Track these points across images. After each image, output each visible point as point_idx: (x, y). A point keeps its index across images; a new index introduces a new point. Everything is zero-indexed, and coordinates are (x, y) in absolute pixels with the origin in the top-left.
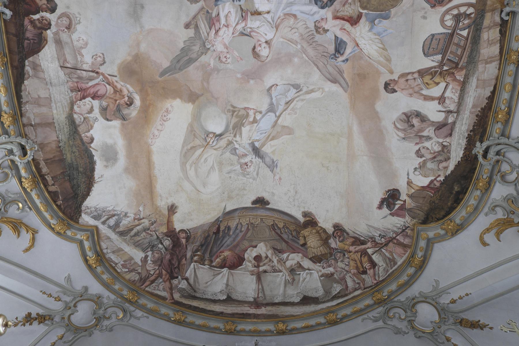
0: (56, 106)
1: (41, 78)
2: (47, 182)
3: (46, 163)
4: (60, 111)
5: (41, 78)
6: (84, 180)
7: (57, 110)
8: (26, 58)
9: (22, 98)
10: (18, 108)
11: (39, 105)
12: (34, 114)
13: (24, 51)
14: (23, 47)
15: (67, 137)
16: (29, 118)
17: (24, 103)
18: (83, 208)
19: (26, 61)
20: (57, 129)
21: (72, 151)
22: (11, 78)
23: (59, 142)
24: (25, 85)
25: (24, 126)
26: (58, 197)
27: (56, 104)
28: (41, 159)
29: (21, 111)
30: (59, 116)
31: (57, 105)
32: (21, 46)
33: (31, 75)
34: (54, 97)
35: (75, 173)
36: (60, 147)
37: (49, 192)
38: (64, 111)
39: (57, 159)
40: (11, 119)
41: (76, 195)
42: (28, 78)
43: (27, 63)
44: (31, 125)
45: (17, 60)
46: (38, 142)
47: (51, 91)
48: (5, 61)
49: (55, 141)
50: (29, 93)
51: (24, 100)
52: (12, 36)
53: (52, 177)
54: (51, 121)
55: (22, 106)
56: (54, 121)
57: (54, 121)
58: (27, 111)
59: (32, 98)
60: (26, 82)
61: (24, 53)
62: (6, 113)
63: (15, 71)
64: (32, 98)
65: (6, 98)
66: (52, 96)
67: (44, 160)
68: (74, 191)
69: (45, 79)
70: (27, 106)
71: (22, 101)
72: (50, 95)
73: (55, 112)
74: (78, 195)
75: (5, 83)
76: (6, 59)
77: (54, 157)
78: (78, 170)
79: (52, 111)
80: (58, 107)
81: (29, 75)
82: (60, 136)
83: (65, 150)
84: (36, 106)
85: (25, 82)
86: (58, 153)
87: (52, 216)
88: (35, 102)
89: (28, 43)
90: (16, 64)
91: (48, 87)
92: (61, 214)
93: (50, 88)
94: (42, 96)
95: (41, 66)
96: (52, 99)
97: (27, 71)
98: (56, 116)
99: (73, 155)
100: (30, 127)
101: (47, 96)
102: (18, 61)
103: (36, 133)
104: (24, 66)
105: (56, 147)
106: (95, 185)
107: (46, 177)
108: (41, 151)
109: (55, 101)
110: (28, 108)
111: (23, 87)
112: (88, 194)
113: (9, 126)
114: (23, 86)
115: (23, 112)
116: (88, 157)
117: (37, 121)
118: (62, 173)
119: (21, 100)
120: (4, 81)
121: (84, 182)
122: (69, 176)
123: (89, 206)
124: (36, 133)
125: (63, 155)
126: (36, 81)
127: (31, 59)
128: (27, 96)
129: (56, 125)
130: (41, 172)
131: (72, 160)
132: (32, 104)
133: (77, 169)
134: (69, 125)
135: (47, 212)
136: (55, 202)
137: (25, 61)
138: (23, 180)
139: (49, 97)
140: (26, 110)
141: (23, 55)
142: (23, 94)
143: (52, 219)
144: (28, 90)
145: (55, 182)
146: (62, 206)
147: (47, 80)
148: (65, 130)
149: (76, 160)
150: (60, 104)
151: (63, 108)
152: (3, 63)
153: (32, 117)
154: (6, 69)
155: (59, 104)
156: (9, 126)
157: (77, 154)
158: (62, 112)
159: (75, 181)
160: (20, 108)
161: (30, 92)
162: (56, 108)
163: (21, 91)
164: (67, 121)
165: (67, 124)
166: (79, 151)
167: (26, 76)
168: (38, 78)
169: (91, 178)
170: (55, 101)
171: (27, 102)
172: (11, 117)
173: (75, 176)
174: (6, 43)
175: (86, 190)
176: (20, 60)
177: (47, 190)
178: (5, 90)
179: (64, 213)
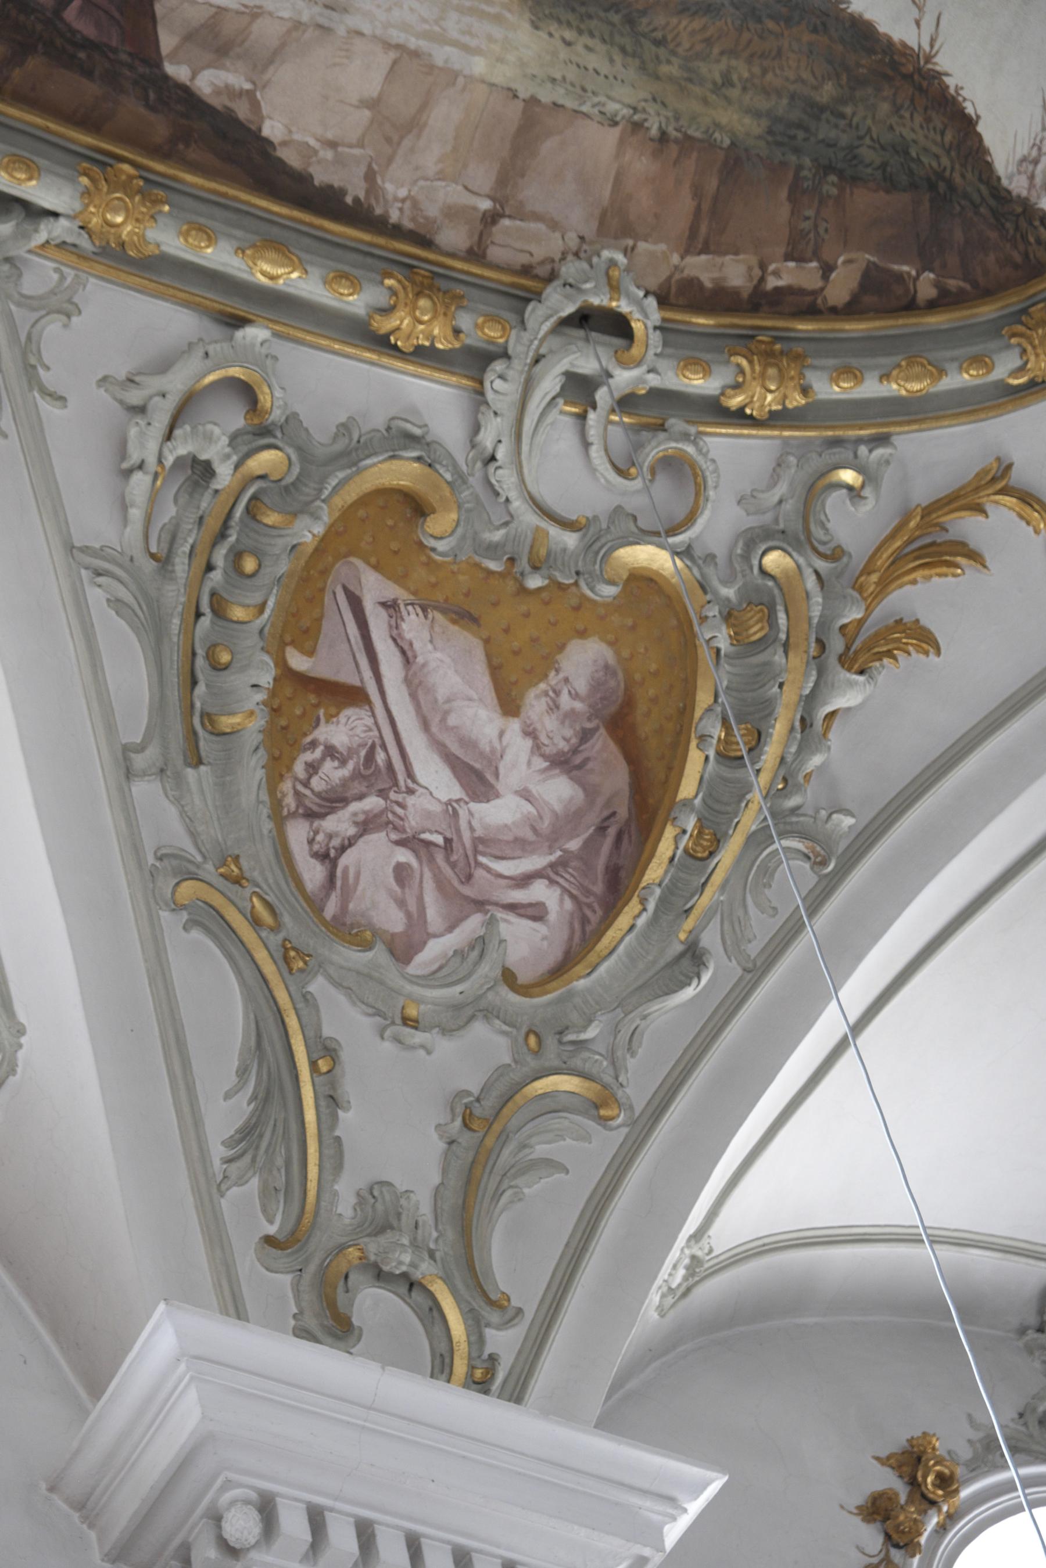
0: (455, 44)
1: (283, 45)
2: (801, 292)
3: (705, 250)
4: (490, 38)
5: (283, 45)
6: (885, 107)
7: (476, 51)
8: (155, 62)
9: (343, 192)
10: (381, 241)
11: (414, 125)
12: (441, 176)
13: (115, 51)
14: (88, 44)
15: (631, 74)
16: (452, 213)
17: (368, 192)
18: (1018, 186)
19: (170, 69)
20: (570, 103)
21: (716, 89)
22: (224, 195)
23: (637, 127)
24: (284, 144)
25: (476, 254)
26: (900, 278)
27: (442, 39)
28: (675, 259)
29: (397, 232)
30: (511, 57)
31: (454, 34)
32: (82, 55)
33: (247, 86)
34: (405, 27)
35: (825, 131)
36: (663, 137)
37: (852, 309)
38: (497, 19)
39: (712, 184)
40: (423, 302)
41: (932, 187)
42: (255, 106)
43: (177, 71)
44: (491, 219)
45: (142, 110)
46: (590, 230)
47: (366, 29)
48: (131, 178)
49: (622, 142)
50: (333, 145)
51: (355, 189)
52: (17, 74)
53: (788, 257)
54: (514, 112)
55: (378, 211)
56: (523, 94)
57: (523, 94)
58: (415, 204)
59: (360, 144)
60: (272, 129)
61: (124, 57)
62: (386, 311)
63: (193, 154)
64: (360, 144)
65: (315, 272)
66: (397, 36)
67: (686, 252)
68: (914, 186)
69: (297, 25)
70: (389, 187)
71: (357, 200)
72: (388, 46)
73: (479, 66)
74: (940, 175)
75: (239, 233)
76: (126, 167)
77: (697, 192)
78: (822, 109)
79: (470, 78)
80: (466, 39)
81: (242, 93)
82: (612, 107)
83: (693, 118)
84: (407, 143)
85: (266, 132)
86: (690, 164)
87: (978, 360)
88: (388, 140)
89: (81, 11)
90: (160, 129)
91: (341, 31)
92: (987, 311)
93: (353, 21)
94: (373, 87)
95: (221, 10)
96: (413, 43)
97: (217, 92)
98: (502, 75)
99: (735, 93)
100: (494, 229)
101: (385, 59)
102: (153, 109)
103: (537, 217)
104: (186, 96)
105: (656, 154)
106: (943, 62)
107: (772, 283)
108: (637, 238)
109: (427, 36)
110: (403, 193)
111: (291, 158)
112: (966, 124)
113: (457, 332)
114: (286, 155)
115: (408, 224)
116: (788, 20)
117: (483, 176)
118: (792, 198)
119: (349, 200)
120: (230, 236)
121: (897, 109)
122: (829, 169)
123: (1022, 150)
124: (537, 217)
125: (709, 145)
126: (283, 74)
127: (167, 41)
128: (340, 161)
129: (546, 95)
130: (735, 292)
131: (757, 114)
132: (390, 160)
133: (817, 110)
134: (580, 32)
135: (942, 372)
136: (910, 306)
137: (166, 78)
138: (735, 402)
139: (393, 55)
140: (408, 204)
141: (131, 67)
142: (321, 176)
143: (990, 369)
144: (312, 142)
145: (816, 255)
146: (953, 284)
147: (305, 18)
148: (593, 61)
149: (766, 92)
150: (453, 16)
151: (482, 15)
152: (140, 191)
153: (452, 194)
154: (172, 188)
155: (453, 23)
156: (457, 332)
157: (742, 69)
158: (498, 32)
159: (867, 154)
160: (380, 225)
161: (330, 135)
162: (465, 48)
163: (303, 178)
164: (553, 27)
165: (568, 35)
166: (733, 53)
167: (242, 111)
168: (275, 56)
169: (894, 65)
170: (427, 36)
171: (370, 176)
172: (418, 295)
173: (844, 140)
174: (39, 121)
175: (938, 122)
176: (152, 95)
177: (835, 312)
178: (272, 255)
179: (985, 293)
